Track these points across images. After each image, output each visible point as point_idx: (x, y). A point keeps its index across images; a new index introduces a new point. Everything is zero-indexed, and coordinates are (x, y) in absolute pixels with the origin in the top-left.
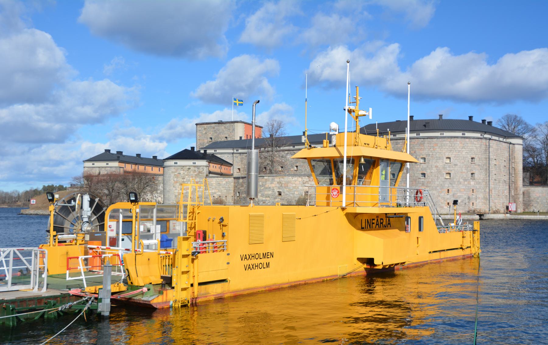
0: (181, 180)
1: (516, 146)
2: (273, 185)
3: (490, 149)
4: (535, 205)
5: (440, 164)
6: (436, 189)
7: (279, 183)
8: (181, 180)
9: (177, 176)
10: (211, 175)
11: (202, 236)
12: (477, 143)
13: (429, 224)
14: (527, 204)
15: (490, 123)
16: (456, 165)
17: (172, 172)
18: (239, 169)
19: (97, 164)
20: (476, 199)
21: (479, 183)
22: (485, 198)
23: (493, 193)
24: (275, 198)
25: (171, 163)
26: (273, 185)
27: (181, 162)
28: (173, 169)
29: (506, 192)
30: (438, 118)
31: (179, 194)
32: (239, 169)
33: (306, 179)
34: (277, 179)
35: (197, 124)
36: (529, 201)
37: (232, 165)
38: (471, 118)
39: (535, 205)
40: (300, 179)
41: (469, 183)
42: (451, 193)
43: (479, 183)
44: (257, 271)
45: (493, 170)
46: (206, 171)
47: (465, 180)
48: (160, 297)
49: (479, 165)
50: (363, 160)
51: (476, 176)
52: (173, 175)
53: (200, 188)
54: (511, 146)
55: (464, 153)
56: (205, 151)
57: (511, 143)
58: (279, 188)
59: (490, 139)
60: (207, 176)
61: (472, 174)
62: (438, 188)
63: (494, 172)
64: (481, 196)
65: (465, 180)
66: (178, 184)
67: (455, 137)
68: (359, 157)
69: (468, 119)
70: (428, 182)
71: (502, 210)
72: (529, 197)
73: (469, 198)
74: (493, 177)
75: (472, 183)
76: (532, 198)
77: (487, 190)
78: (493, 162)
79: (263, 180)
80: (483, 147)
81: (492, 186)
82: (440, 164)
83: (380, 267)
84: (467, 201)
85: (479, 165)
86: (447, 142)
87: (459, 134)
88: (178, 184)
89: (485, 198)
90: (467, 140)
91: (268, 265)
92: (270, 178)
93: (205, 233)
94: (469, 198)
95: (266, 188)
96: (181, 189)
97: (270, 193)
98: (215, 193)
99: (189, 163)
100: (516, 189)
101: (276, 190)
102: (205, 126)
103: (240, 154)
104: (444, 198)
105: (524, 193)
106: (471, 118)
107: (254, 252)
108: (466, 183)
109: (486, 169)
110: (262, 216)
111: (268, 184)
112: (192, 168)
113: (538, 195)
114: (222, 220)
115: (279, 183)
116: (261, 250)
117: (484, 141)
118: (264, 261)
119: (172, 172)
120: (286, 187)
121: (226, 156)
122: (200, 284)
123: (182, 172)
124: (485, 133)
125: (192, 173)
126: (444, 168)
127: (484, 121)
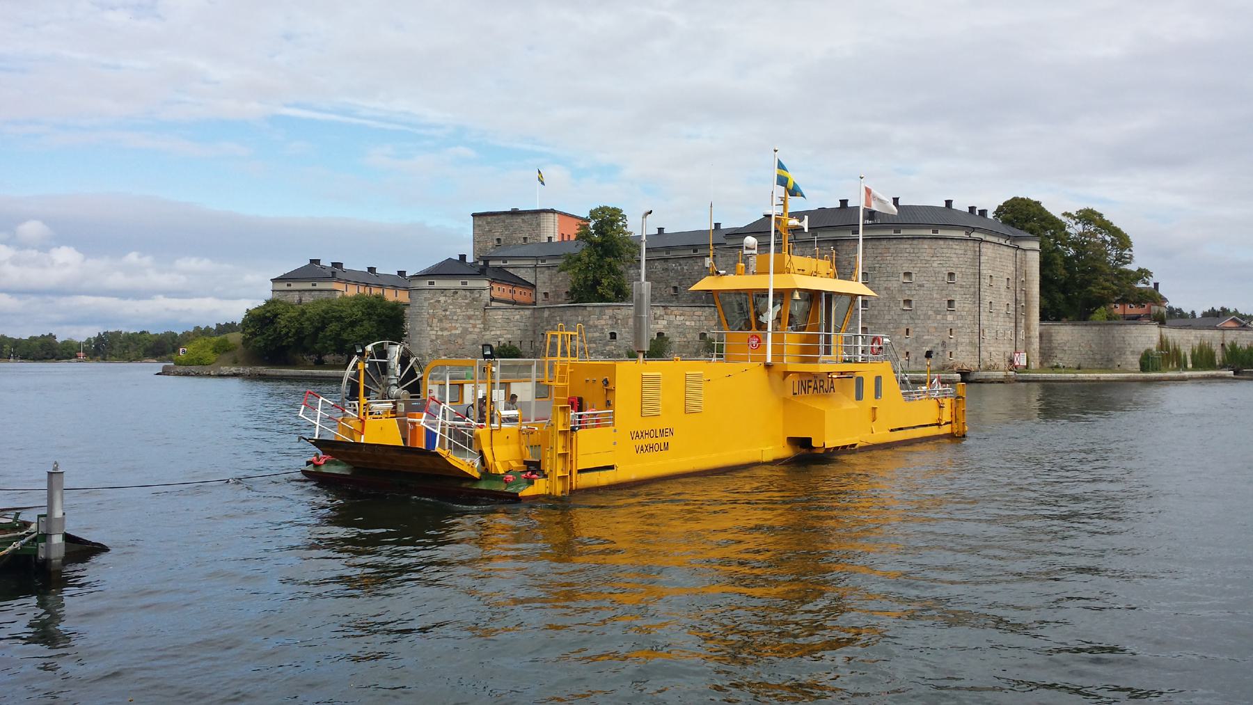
0: (440, 313)
1: (1029, 253)
2: (603, 322)
4: (1060, 356)
5: (894, 284)
6: (885, 329)
7: (613, 317)
8: (440, 313)
9: (434, 307)
10: (494, 304)
11: (576, 405)
12: (958, 248)
13: (891, 386)
14: (1047, 353)
16: (921, 286)
17: (426, 299)
18: (546, 294)
20: (956, 345)
21: (961, 317)
23: (988, 335)
24: (606, 345)
25: (425, 284)
26: (603, 322)
27: (439, 284)
28: (427, 295)
29: (1010, 333)
31: (437, 337)
32: (546, 294)
33: (659, 312)
34: (609, 312)
36: (1051, 349)
37: (534, 286)
38: (949, 203)
39: (1060, 356)
42: (911, 335)
43: (961, 317)
44: (652, 454)
45: (987, 297)
46: (486, 295)
48: (531, 487)
49: (962, 286)
50: (797, 296)
52: (426, 304)
53: (474, 326)
55: (935, 265)
56: (486, 262)
57: (1018, 248)
58: (612, 326)
59: (982, 240)
61: (950, 302)
62: (890, 326)
63: (988, 299)
64: (966, 340)
65: (937, 312)
66: (435, 321)
68: (792, 291)
70: (872, 316)
71: (1003, 364)
72: (1050, 341)
73: (944, 343)
74: (985, 305)
75: (950, 318)
76: (1055, 344)
78: (985, 282)
79: (585, 313)
81: (984, 322)
82: (894, 284)
83: (821, 451)
84: (940, 349)
85: (962, 286)
86: (906, 245)
87: (929, 233)
88: (435, 321)
90: (941, 242)
91: (666, 447)
92: (597, 310)
93: (580, 400)
94: (944, 343)
95: (591, 327)
96: (442, 330)
97: (597, 334)
98: (501, 336)
99: (457, 284)
100: (1027, 328)
101: (607, 331)
103: (548, 267)
104: (900, 344)
105: (1041, 336)
106: (949, 203)
107: (648, 429)
108: (939, 317)
110: (658, 377)
111: (593, 320)
112: (459, 292)
113: (1065, 338)
114: (606, 382)
115: (613, 317)
116: (658, 424)
117: (970, 244)
118: (661, 440)
119: (426, 299)
121: (523, 271)
122: (580, 471)
123: (442, 299)
124: (974, 229)
125: (460, 300)
126: (901, 291)
127: (972, 209)
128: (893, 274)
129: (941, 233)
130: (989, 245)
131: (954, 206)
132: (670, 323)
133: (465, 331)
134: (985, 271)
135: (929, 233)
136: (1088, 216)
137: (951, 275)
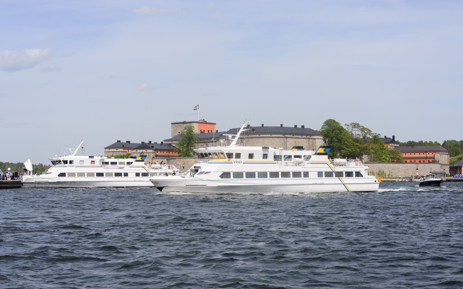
15: (303, 127)
19: (111, 150)
34: (182, 160)
35: (172, 124)
40: (194, 160)
59: (287, 138)
60: (153, 158)
67: (266, 137)
69: (280, 126)
80: (282, 142)
86: (260, 139)
87: (269, 135)
101: (182, 166)
102: (176, 125)
115: (183, 162)
120: (187, 164)
127: (296, 126)
129: (273, 135)
131: (283, 126)
135: (269, 135)
136: (355, 125)
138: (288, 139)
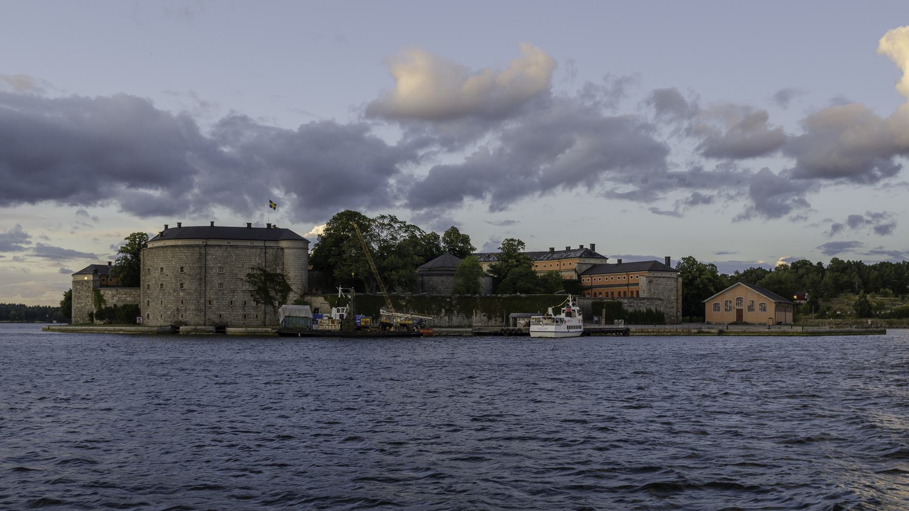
3: (209, 257)
20: (186, 310)
22: (197, 309)
30: (176, 226)
38: (212, 223)
41: (178, 294)
47: (175, 291)
49: (190, 275)
51: (185, 286)
54: (270, 251)
63: (216, 281)
64: (192, 307)
65: (175, 291)
73: (178, 309)
75: (182, 294)
77: (202, 301)
81: (211, 295)
85: (190, 275)
89: (197, 309)
94: (178, 309)
109: (200, 279)
128: (156, 269)
130: (217, 249)
131: (215, 225)
132: (119, 299)
133: (86, 305)
134: (210, 264)
137: (182, 268)
138: (211, 251)
